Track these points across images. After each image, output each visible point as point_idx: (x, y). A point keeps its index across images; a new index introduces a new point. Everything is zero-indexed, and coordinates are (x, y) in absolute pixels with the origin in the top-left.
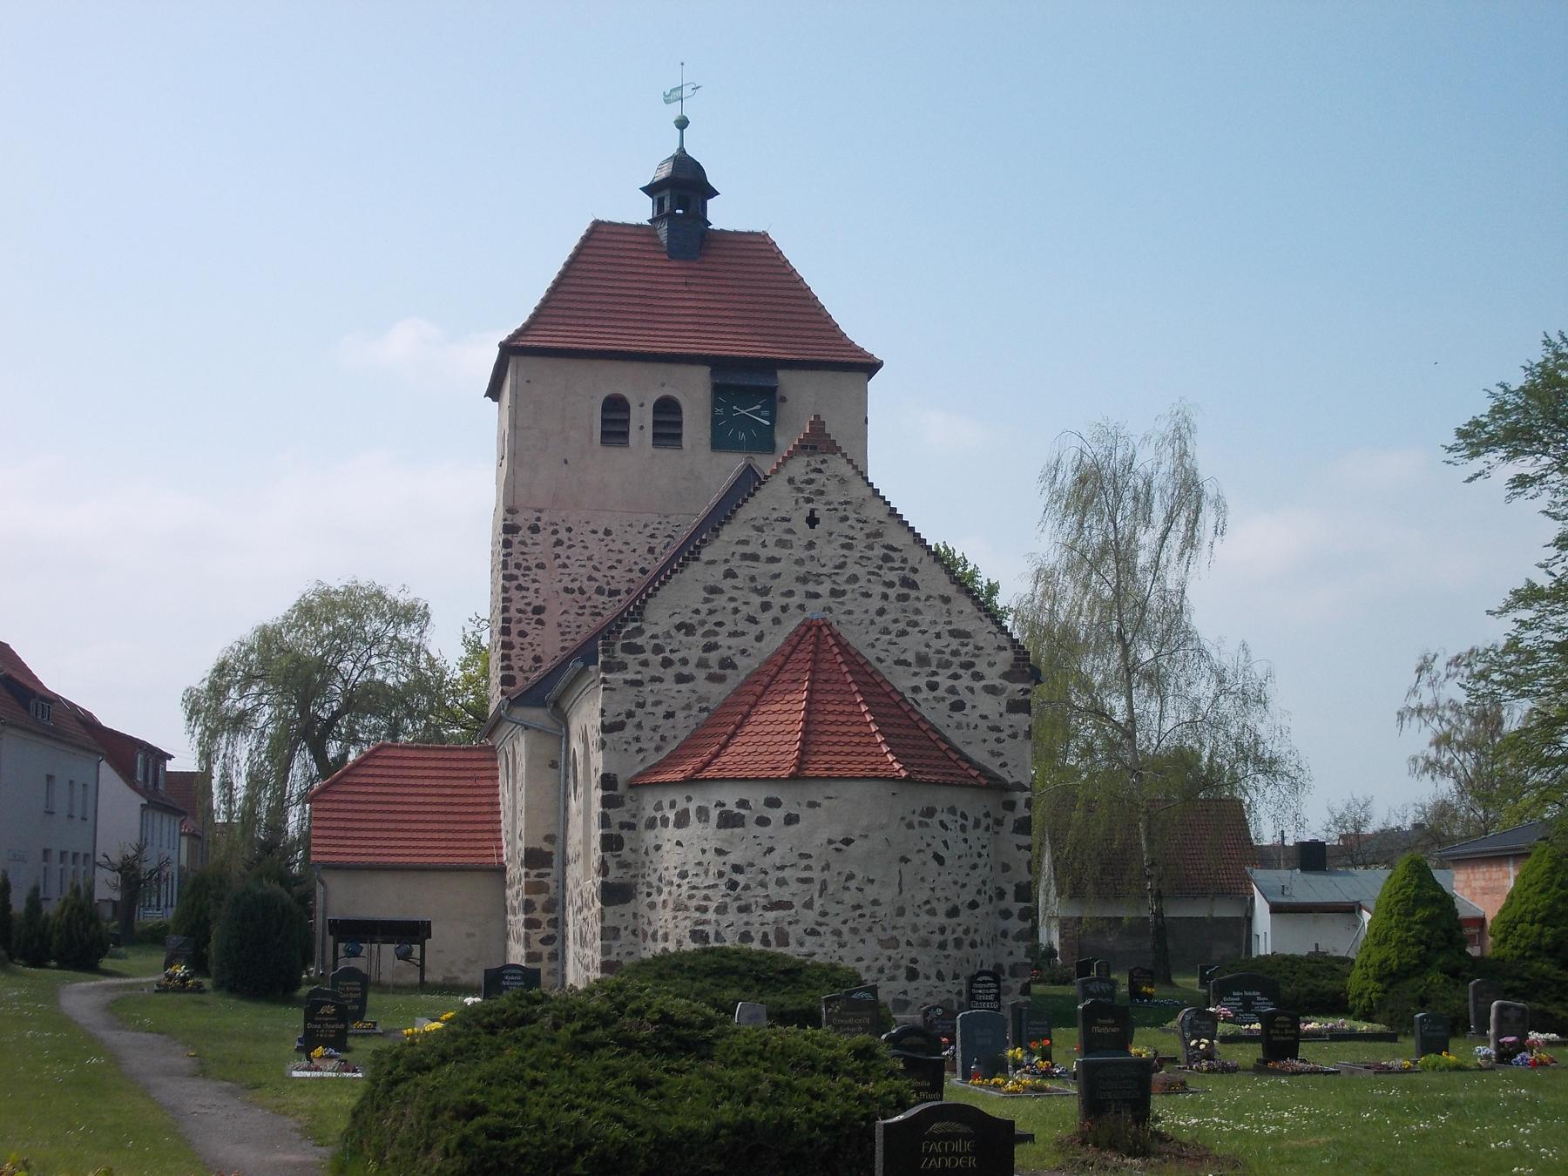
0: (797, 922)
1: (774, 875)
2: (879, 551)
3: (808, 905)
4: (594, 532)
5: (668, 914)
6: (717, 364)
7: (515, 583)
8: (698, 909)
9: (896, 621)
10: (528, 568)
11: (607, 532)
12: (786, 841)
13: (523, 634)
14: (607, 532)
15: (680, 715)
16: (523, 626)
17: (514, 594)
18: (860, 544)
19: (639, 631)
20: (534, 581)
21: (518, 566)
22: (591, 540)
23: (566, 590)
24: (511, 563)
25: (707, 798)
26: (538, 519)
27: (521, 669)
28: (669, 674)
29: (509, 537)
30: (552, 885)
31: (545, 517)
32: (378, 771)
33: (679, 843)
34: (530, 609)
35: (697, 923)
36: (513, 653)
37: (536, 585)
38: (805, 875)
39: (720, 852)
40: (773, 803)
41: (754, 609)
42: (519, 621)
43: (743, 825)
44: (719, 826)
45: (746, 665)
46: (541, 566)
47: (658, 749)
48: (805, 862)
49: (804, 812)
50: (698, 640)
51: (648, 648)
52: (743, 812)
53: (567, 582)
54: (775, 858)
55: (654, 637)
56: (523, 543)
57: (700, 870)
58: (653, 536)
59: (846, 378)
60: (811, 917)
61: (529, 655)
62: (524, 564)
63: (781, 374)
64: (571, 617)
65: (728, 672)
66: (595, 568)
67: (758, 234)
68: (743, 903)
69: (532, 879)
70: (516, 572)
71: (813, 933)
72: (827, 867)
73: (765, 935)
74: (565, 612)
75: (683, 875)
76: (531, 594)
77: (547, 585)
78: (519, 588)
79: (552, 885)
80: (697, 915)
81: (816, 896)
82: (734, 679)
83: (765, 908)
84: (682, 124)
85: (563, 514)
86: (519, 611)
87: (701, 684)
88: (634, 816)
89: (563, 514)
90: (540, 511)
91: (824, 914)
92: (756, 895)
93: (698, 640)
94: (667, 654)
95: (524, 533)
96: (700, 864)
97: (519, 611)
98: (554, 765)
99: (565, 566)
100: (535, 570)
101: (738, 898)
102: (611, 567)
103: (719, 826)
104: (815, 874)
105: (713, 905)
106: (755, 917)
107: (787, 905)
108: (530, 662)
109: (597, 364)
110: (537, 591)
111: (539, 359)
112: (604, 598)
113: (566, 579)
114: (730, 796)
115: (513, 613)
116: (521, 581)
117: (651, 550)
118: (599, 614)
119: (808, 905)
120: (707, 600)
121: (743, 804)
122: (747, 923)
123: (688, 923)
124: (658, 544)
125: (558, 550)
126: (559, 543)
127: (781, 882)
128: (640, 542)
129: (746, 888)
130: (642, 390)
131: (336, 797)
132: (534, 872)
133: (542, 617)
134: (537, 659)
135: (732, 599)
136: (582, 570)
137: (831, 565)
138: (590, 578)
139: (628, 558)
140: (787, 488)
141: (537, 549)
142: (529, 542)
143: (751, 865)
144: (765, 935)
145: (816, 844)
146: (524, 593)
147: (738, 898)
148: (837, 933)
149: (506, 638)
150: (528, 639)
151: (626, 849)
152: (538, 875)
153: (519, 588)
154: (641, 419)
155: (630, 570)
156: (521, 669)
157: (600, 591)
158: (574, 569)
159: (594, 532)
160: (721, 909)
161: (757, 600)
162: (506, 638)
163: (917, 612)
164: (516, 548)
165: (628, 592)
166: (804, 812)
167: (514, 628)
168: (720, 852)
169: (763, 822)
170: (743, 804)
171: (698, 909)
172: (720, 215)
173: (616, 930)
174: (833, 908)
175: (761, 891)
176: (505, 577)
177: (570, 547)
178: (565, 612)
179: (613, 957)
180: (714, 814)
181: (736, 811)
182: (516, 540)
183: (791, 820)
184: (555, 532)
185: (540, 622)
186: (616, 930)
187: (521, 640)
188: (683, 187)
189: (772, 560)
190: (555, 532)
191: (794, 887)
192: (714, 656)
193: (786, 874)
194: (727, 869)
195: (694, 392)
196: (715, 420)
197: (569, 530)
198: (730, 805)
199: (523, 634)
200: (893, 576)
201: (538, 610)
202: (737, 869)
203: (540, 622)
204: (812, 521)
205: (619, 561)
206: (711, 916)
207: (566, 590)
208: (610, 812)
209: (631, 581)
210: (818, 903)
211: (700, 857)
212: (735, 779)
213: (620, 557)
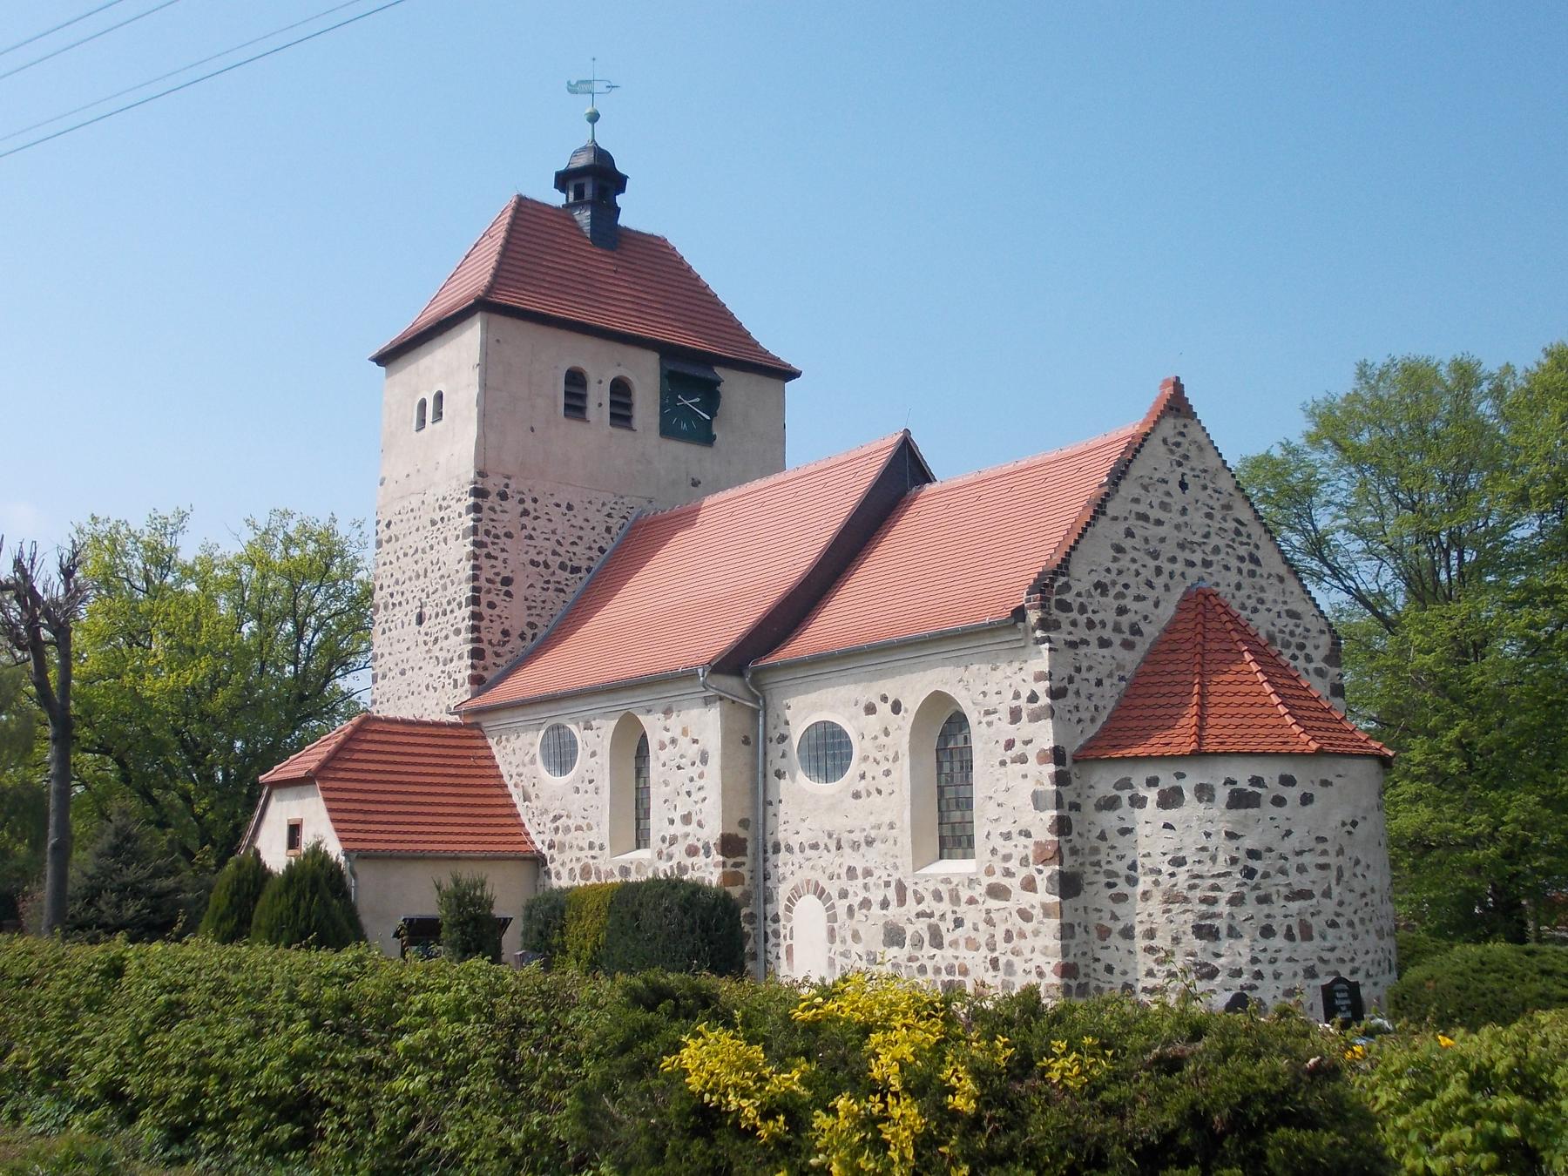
0: (1319, 912)
1: (1294, 861)
2: (1231, 525)
3: (1327, 894)
4: (558, 505)
5: (1155, 905)
6: (667, 352)
7: (485, 551)
8: (1204, 901)
9: (1249, 597)
10: (497, 537)
11: (570, 507)
12: (1303, 821)
13: (492, 605)
14: (570, 507)
15: (1107, 682)
16: (492, 597)
17: (484, 562)
18: (1218, 515)
19: (1066, 587)
20: (503, 550)
21: (487, 533)
22: (556, 514)
23: (533, 563)
24: (481, 531)
25: (1217, 775)
26: (507, 486)
27: (490, 642)
28: (1092, 636)
29: (479, 501)
30: (747, 875)
31: (513, 485)
32: (373, 747)
33: (1167, 826)
34: (498, 579)
35: (1203, 916)
36: (483, 624)
37: (505, 555)
38: (1322, 860)
39: (1231, 836)
40: (1287, 781)
41: (1148, 573)
42: (489, 591)
43: (1258, 806)
44: (1230, 806)
45: (1151, 631)
46: (509, 535)
47: (1093, 720)
48: (1321, 847)
49: (1318, 792)
50: (1110, 602)
51: (1075, 606)
52: (1259, 790)
53: (533, 555)
54: (1293, 843)
55: (1079, 595)
56: (492, 509)
57: (1204, 856)
58: (609, 515)
59: (769, 384)
60: (1329, 907)
61: (497, 627)
62: (493, 531)
63: (720, 372)
64: (537, 591)
65: (1137, 638)
66: (559, 542)
67: (658, 238)
68: (1261, 893)
69: (729, 869)
70: (485, 539)
71: (1333, 925)
72: (1340, 852)
73: (1289, 928)
74: (531, 586)
75: (1179, 862)
76: (499, 563)
77: (515, 557)
78: (489, 556)
79: (747, 875)
80: (1204, 907)
81: (1334, 882)
82: (1143, 645)
83: (1287, 898)
84: (594, 118)
85: (530, 483)
86: (489, 581)
87: (1117, 650)
88: (1079, 795)
89: (530, 483)
90: (509, 478)
91: (1341, 904)
92: (1276, 885)
93: (1110, 602)
94: (1090, 614)
95: (493, 499)
96: (1204, 849)
97: (489, 581)
98: (746, 741)
99: (531, 537)
100: (504, 539)
101: (1256, 887)
102: (573, 543)
103: (1230, 806)
104: (1331, 859)
105: (1224, 896)
106: (1277, 907)
107: (1305, 895)
108: (499, 636)
109: (561, 333)
110: (505, 561)
111: (520, 323)
112: (567, 574)
113: (533, 552)
114: (1242, 773)
115: (482, 583)
116: (490, 549)
117: (608, 530)
118: (562, 591)
119: (1327, 894)
120: (1115, 560)
121: (1257, 781)
122: (1268, 916)
123: (1190, 917)
124: (615, 523)
125: (525, 520)
126: (525, 513)
127: (1301, 869)
128: (598, 520)
129: (1266, 875)
130: (603, 366)
131: (341, 775)
132: (731, 861)
133: (510, 588)
134: (505, 633)
135: (1134, 561)
136: (547, 544)
137: (1200, 533)
138: (555, 553)
139: (589, 536)
140: (1162, 449)
141: (506, 517)
142: (498, 508)
143: (1270, 850)
144: (1289, 928)
145: (1331, 826)
146: (493, 562)
147: (1256, 887)
148: (1351, 924)
149: (477, 609)
150: (497, 611)
151: (1074, 833)
152: (736, 865)
153: (489, 556)
154: (598, 397)
155: (590, 548)
156: (490, 642)
157: (563, 566)
158: (539, 542)
159: (558, 505)
160: (1237, 900)
161: (1152, 564)
162: (477, 609)
163: (1262, 589)
164: (486, 514)
165: (589, 570)
166: (1318, 792)
167: (484, 601)
168: (1231, 836)
169: (1279, 801)
170: (1257, 781)
171: (1204, 901)
172: (633, 212)
173: (1072, 926)
174: (1348, 897)
175: (1281, 879)
176: (475, 543)
177: (536, 518)
178: (531, 586)
179: (1071, 959)
180: (1222, 794)
181: (1250, 789)
182: (486, 505)
183: (1306, 799)
184: (522, 501)
185: (508, 594)
186: (1072, 926)
187: (490, 611)
188: (597, 180)
189: (1159, 523)
190: (522, 501)
191: (1314, 873)
192: (1125, 621)
193: (1307, 859)
194: (1241, 855)
195: (645, 374)
196: (663, 407)
197: (535, 501)
198: (1243, 783)
199: (492, 605)
200: (1243, 551)
201: (507, 581)
202: (1253, 854)
203: (508, 594)
204: (1183, 486)
205: (580, 538)
206: (1223, 908)
207: (533, 563)
208: (1062, 789)
209: (591, 559)
210: (1336, 891)
211: (1203, 841)
212: (1238, 753)
213: (581, 533)
